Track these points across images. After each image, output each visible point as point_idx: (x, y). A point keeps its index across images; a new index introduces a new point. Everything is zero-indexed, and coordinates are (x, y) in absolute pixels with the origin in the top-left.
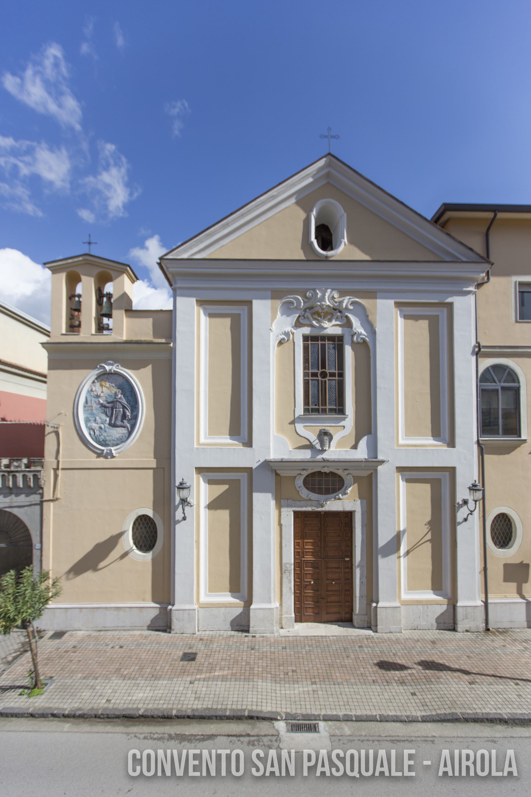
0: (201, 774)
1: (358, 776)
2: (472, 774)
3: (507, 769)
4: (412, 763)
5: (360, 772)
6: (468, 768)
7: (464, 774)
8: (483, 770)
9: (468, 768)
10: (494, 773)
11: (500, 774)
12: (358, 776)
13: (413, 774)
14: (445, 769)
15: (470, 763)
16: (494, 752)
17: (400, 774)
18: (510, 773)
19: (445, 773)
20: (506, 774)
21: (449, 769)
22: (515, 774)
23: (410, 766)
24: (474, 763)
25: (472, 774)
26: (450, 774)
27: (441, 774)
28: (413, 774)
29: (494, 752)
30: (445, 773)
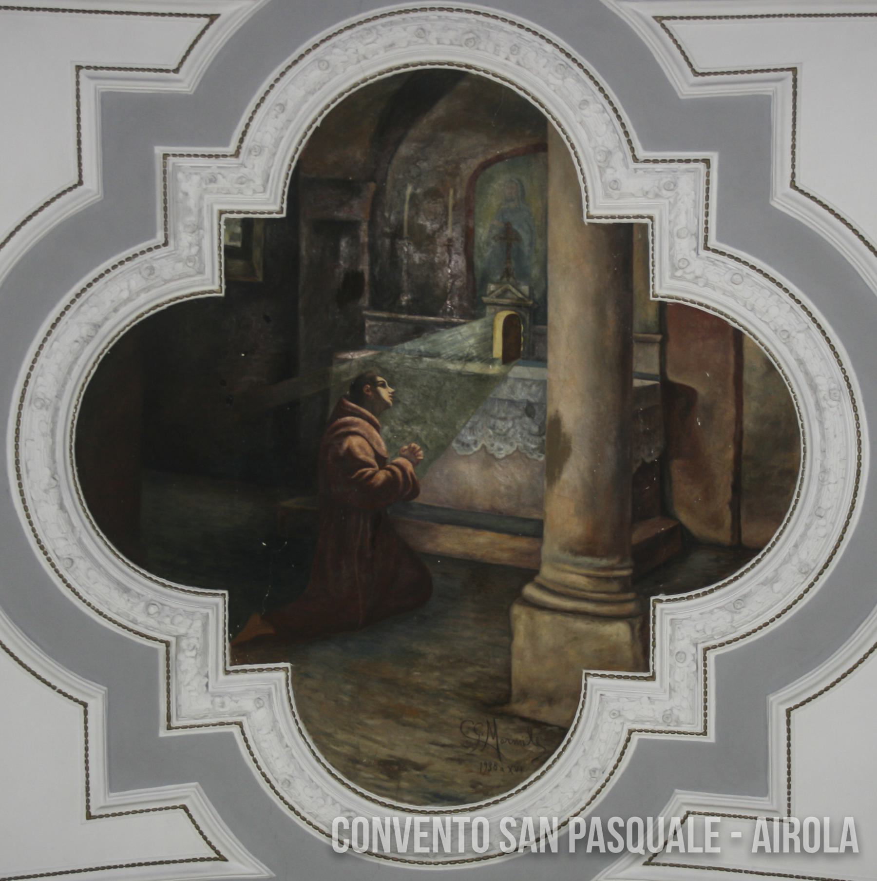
0: (431, 851)
1: (642, 852)
2: (797, 849)
3: (844, 843)
4: (716, 834)
5: (646, 848)
6: (791, 841)
7: (786, 849)
8: (812, 845)
9: (791, 841)
10: (828, 849)
11: (835, 850)
12: (642, 852)
13: (717, 850)
14: (761, 844)
15: (794, 836)
16: (827, 820)
17: (700, 850)
18: (849, 849)
19: (761, 849)
20: (842, 850)
21: (766, 843)
22: (856, 850)
23: (713, 839)
24: (800, 835)
25: (797, 849)
26: (768, 850)
27: (755, 850)
28: (717, 850)
29: (827, 820)
30: (761, 849)
